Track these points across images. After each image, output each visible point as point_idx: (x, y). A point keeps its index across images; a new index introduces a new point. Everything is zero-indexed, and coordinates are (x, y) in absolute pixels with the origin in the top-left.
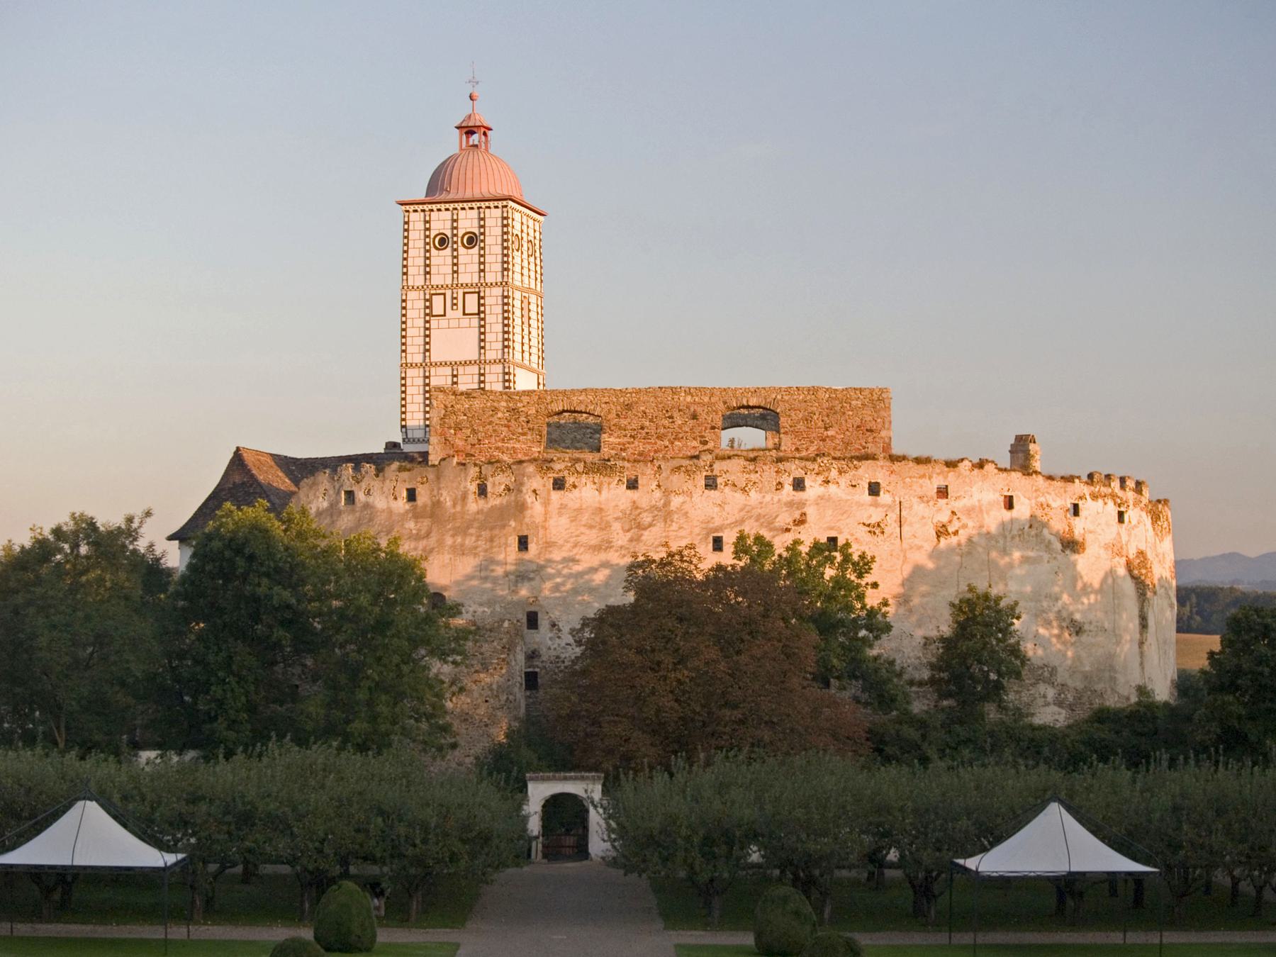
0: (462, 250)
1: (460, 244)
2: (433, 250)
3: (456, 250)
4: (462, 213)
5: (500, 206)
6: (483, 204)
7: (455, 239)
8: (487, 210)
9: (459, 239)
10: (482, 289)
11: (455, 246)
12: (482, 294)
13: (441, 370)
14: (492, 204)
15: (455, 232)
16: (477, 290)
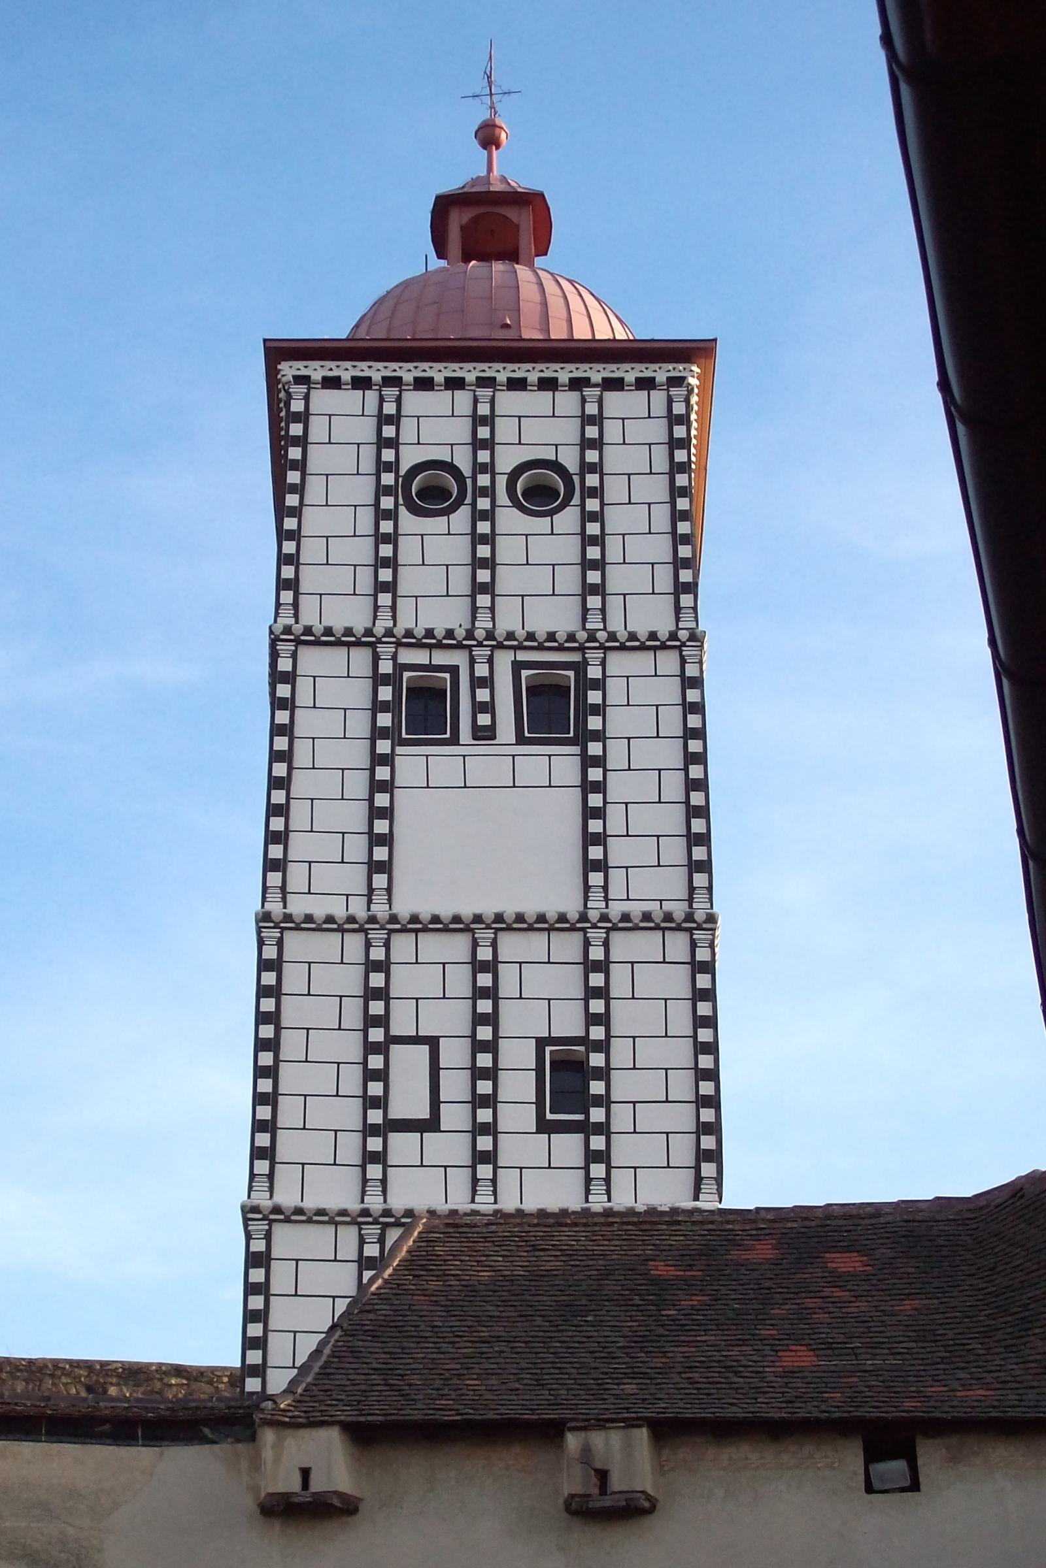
0: (510, 519)
1: (502, 497)
2: (403, 510)
3: (488, 516)
4: (509, 402)
5: (661, 377)
6: (597, 372)
7: (484, 480)
8: (611, 397)
9: (502, 482)
10: (594, 656)
11: (484, 504)
12: (594, 672)
13: (435, 946)
14: (630, 372)
15: (484, 456)
16: (575, 657)
